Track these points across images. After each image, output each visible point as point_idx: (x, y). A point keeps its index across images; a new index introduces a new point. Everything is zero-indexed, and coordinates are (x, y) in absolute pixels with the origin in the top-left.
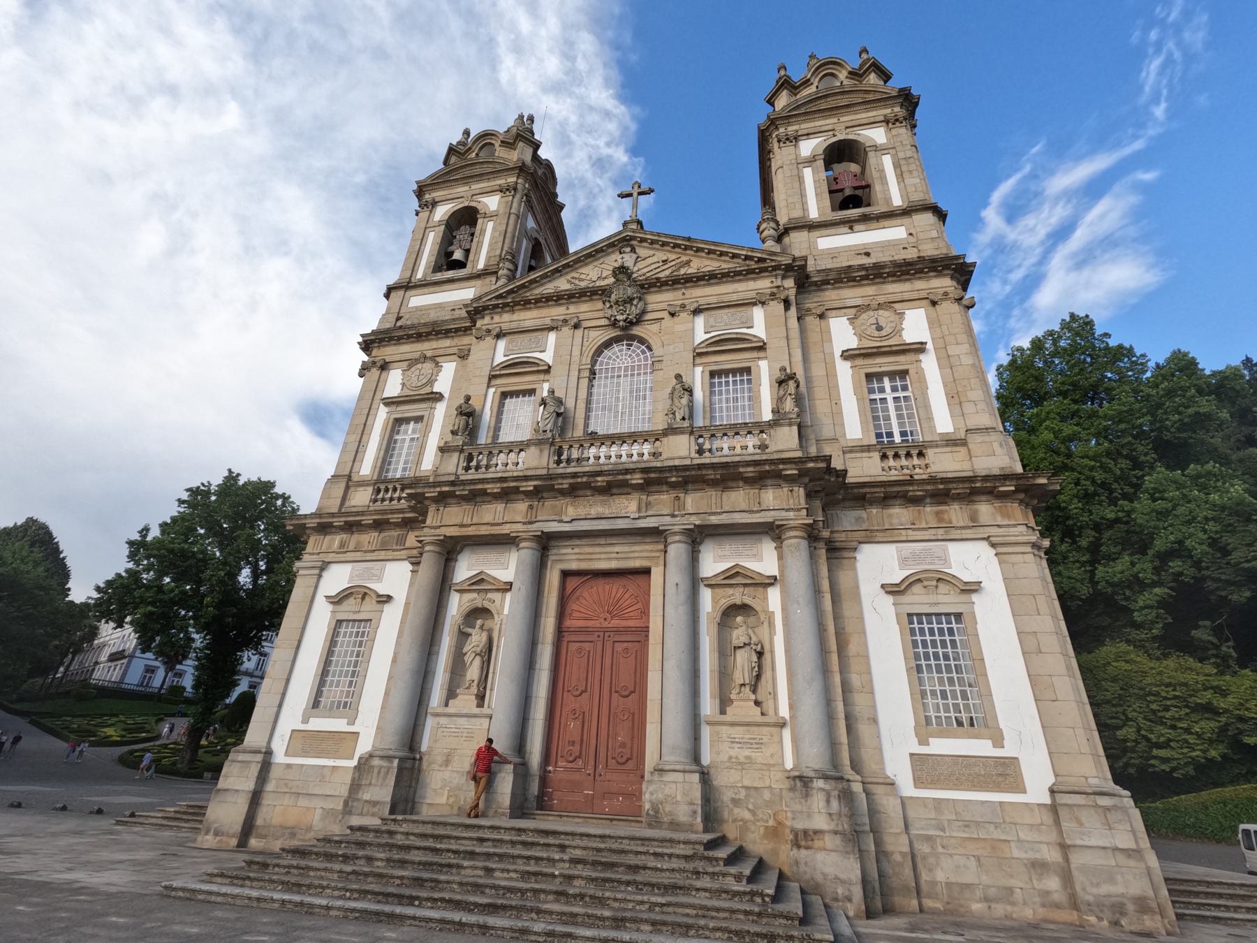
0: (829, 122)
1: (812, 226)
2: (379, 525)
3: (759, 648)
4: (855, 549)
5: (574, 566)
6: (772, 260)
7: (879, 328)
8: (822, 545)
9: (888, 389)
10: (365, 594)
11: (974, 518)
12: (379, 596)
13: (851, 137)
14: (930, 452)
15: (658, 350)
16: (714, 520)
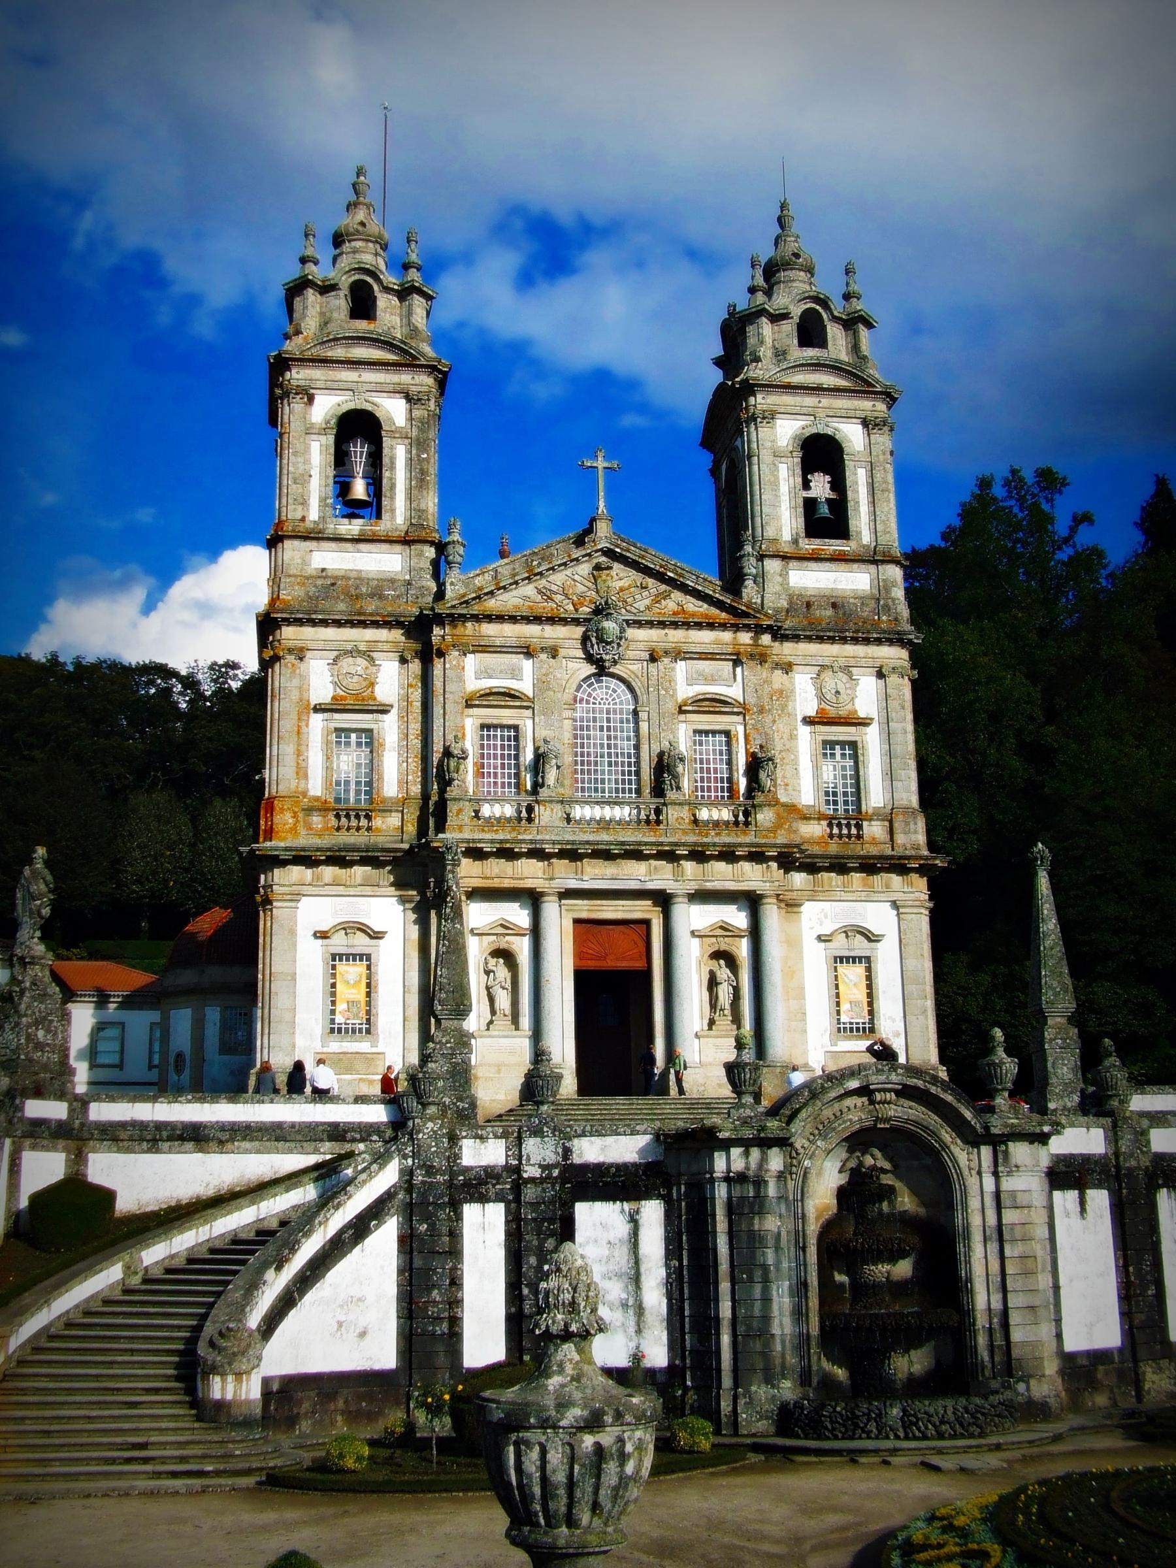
0: (810, 401)
1: (785, 558)
2: (364, 861)
3: (735, 984)
4: (800, 905)
5: (584, 915)
6: (755, 617)
7: (838, 692)
8: (783, 905)
9: (838, 757)
10: (363, 929)
11: (887, 886)
12: (379, 932)
13: (829, 432)
14: (865, 824)
15: (643, 698)
16: (709, 886)
